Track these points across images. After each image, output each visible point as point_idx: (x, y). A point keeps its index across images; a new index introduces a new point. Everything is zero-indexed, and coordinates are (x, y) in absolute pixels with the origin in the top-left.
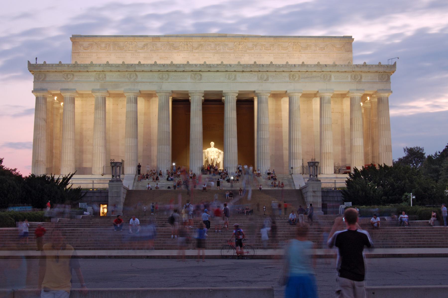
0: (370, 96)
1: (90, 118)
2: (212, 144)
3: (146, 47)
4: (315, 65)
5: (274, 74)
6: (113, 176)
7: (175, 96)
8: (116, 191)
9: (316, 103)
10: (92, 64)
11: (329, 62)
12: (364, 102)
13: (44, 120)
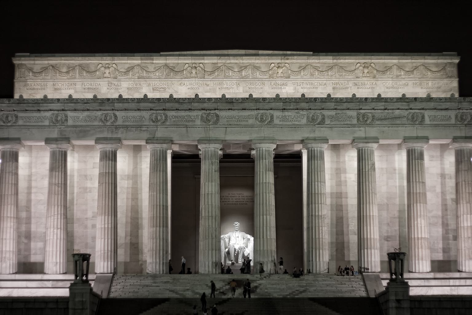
3: (131, 73)
5: (333, 113)
6: (76, 276)
8: (81, 299)
10: (45, 100)
11: (421, 93)
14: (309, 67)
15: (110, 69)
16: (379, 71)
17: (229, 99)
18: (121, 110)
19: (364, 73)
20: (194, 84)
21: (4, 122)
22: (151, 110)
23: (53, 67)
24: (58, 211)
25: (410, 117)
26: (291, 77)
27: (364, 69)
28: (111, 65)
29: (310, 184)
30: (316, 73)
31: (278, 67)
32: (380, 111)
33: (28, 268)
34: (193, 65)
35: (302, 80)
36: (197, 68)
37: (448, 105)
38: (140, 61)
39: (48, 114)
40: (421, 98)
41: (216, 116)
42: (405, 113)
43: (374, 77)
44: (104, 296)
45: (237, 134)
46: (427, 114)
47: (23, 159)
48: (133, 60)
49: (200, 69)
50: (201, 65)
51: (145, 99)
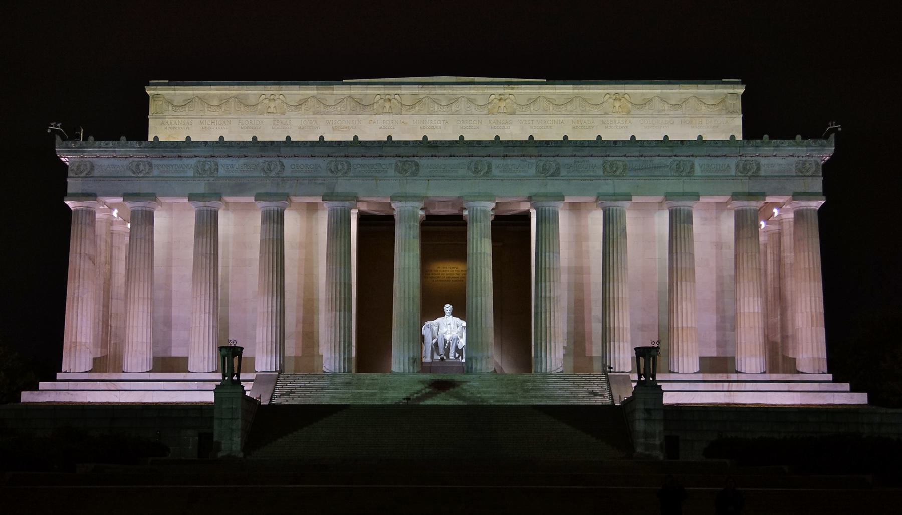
0: (779, 206)
2: (448, 308)
3: (303, 107)
5: (570, 161)
6: (224, 376)
12: (767, 220)
13: (90, 258)
21: (134, 173)
23: (200, 98)
25: (674, 166)
26: (517, 112)
39: (193, 162)
43: (629, 113)
46: (697, 162)
48: (307, 89)
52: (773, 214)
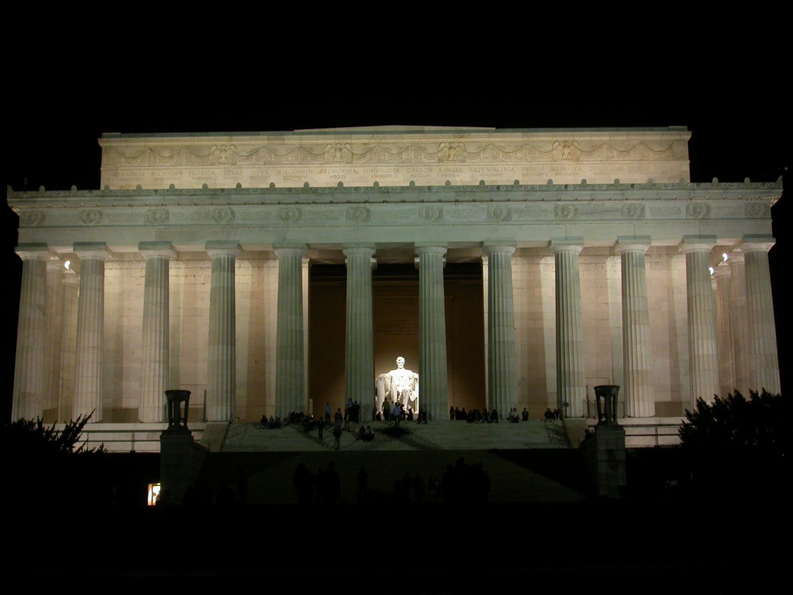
0: (728, 249)
1: (137, 304)
2: (401, 360)
3: (254, 157)
4: (609, 186)
7: (316, 256)
9: (613, 269)
10: (139, 192)
11: (639, 178)
12: (715, 266)
13: (40, 309)
14: (491, 146)
15: (227, 152)
16: (584, 151)
17: (383, 189)
18: (240, 204)
19: (564, 155)
20: (339, 171)
21: (85, 222)
22: (279, 203)
23: (151, 150)
24: (156, 339)
25: (625, 210)
26: (468, 160)
27: (564, 149)
28: (229, 147)
29: (493, 300)
30: (501, 156)
31: (450, 148)
32: (585, 202)
33: (118, 413)
34: (338, 146)
35: (482, 165)
36: (343, 150)
37: (677, 193)
38: (267, 142)
39: (143, 210)
40: (639, 184)
41: (366, 210)
42: (619, 205)
43: (577, 160)
44: (215, 449)
45: (393, 233)
46: (648, 205)
47: (112, 274)
48: (259, 140)
49: (347, 151)
50: (348, 146)
51: (272, 188)
52: (723, 258)
